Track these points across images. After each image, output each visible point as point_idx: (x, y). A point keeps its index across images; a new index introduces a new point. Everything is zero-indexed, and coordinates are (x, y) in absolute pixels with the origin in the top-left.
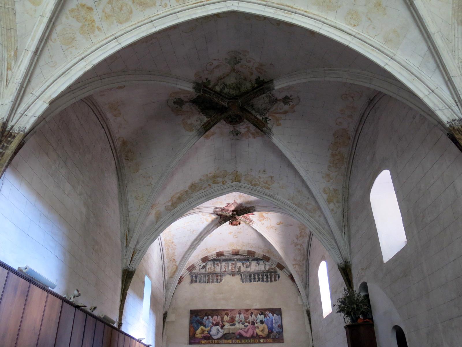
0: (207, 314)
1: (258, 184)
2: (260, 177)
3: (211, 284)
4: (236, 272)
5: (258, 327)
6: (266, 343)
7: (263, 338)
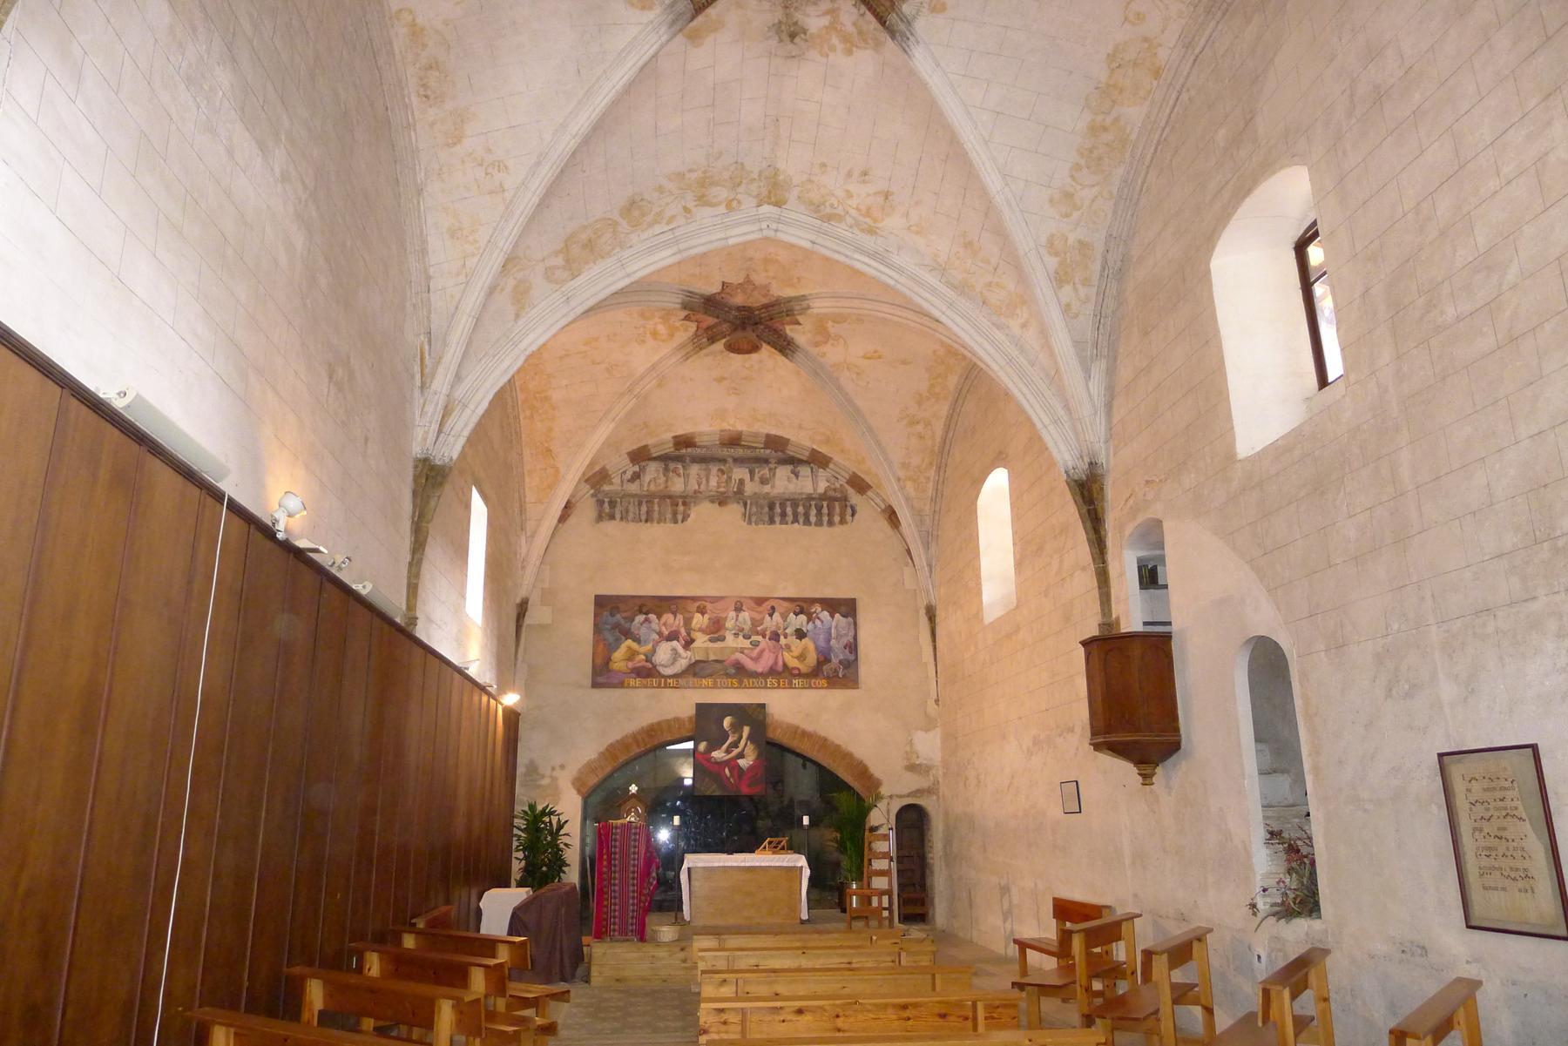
0: (644, 610)
1: (840, 215)
2: (849, 195)
4: (730, 494)
5: (788, 647)
6: (810, 687)
7: (800, 675)
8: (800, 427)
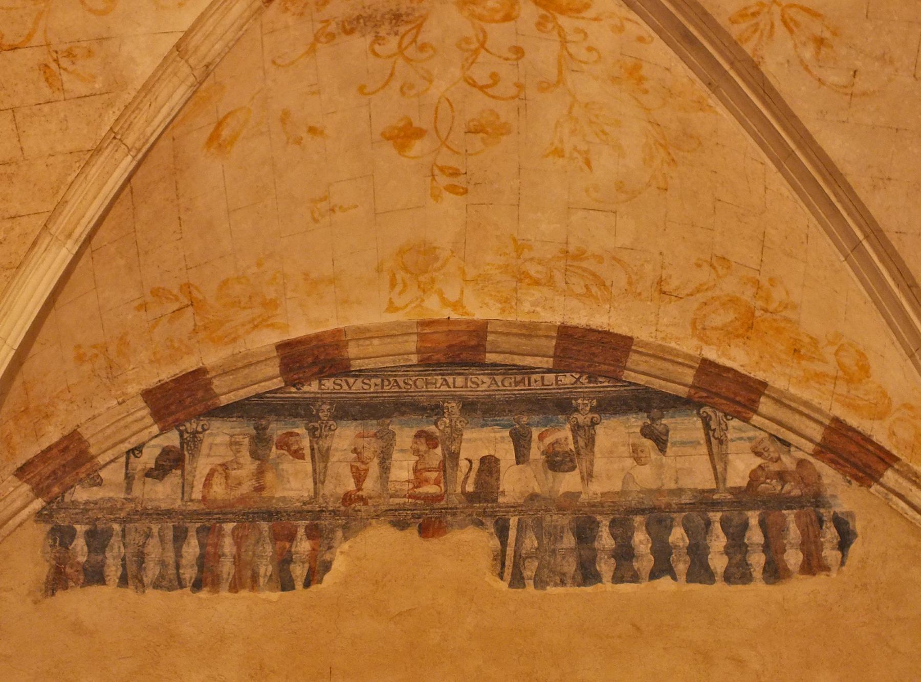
3: (225, 593)
8: (661, 290)
